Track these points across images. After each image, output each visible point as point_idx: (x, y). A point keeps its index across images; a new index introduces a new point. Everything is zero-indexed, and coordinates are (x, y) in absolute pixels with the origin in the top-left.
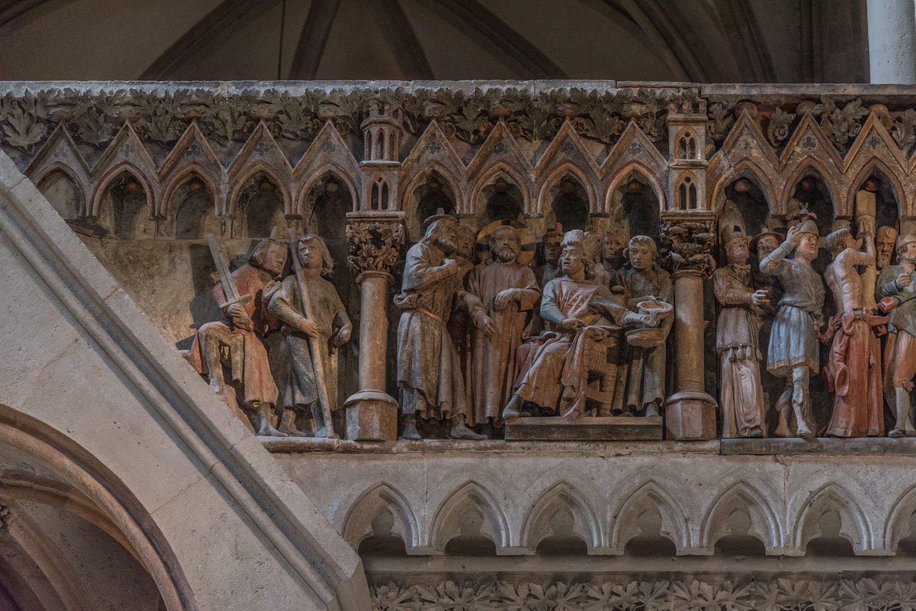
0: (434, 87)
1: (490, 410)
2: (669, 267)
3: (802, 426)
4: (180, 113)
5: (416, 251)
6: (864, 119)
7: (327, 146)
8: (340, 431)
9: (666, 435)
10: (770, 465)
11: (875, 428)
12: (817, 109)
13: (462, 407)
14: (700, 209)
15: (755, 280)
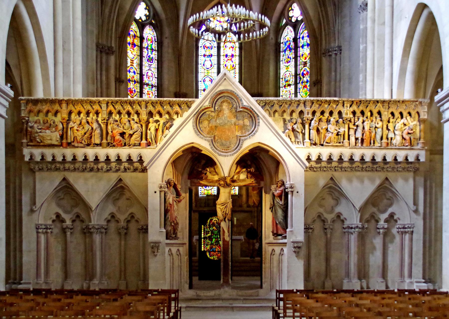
0: (315, 98)
1: (322, 143)
2: (344, 123)
3: (360, 145)
4: (282, 102)
5: (313, 122)
6: (369, 103)
7: (301, 106)
8: (304, 145)
9: (343, 146)
10: (355, 150)
11: (369, 145)
12: (364, 102)
13: (319, 142)
14: (348, 116)
15: (354, 125)
